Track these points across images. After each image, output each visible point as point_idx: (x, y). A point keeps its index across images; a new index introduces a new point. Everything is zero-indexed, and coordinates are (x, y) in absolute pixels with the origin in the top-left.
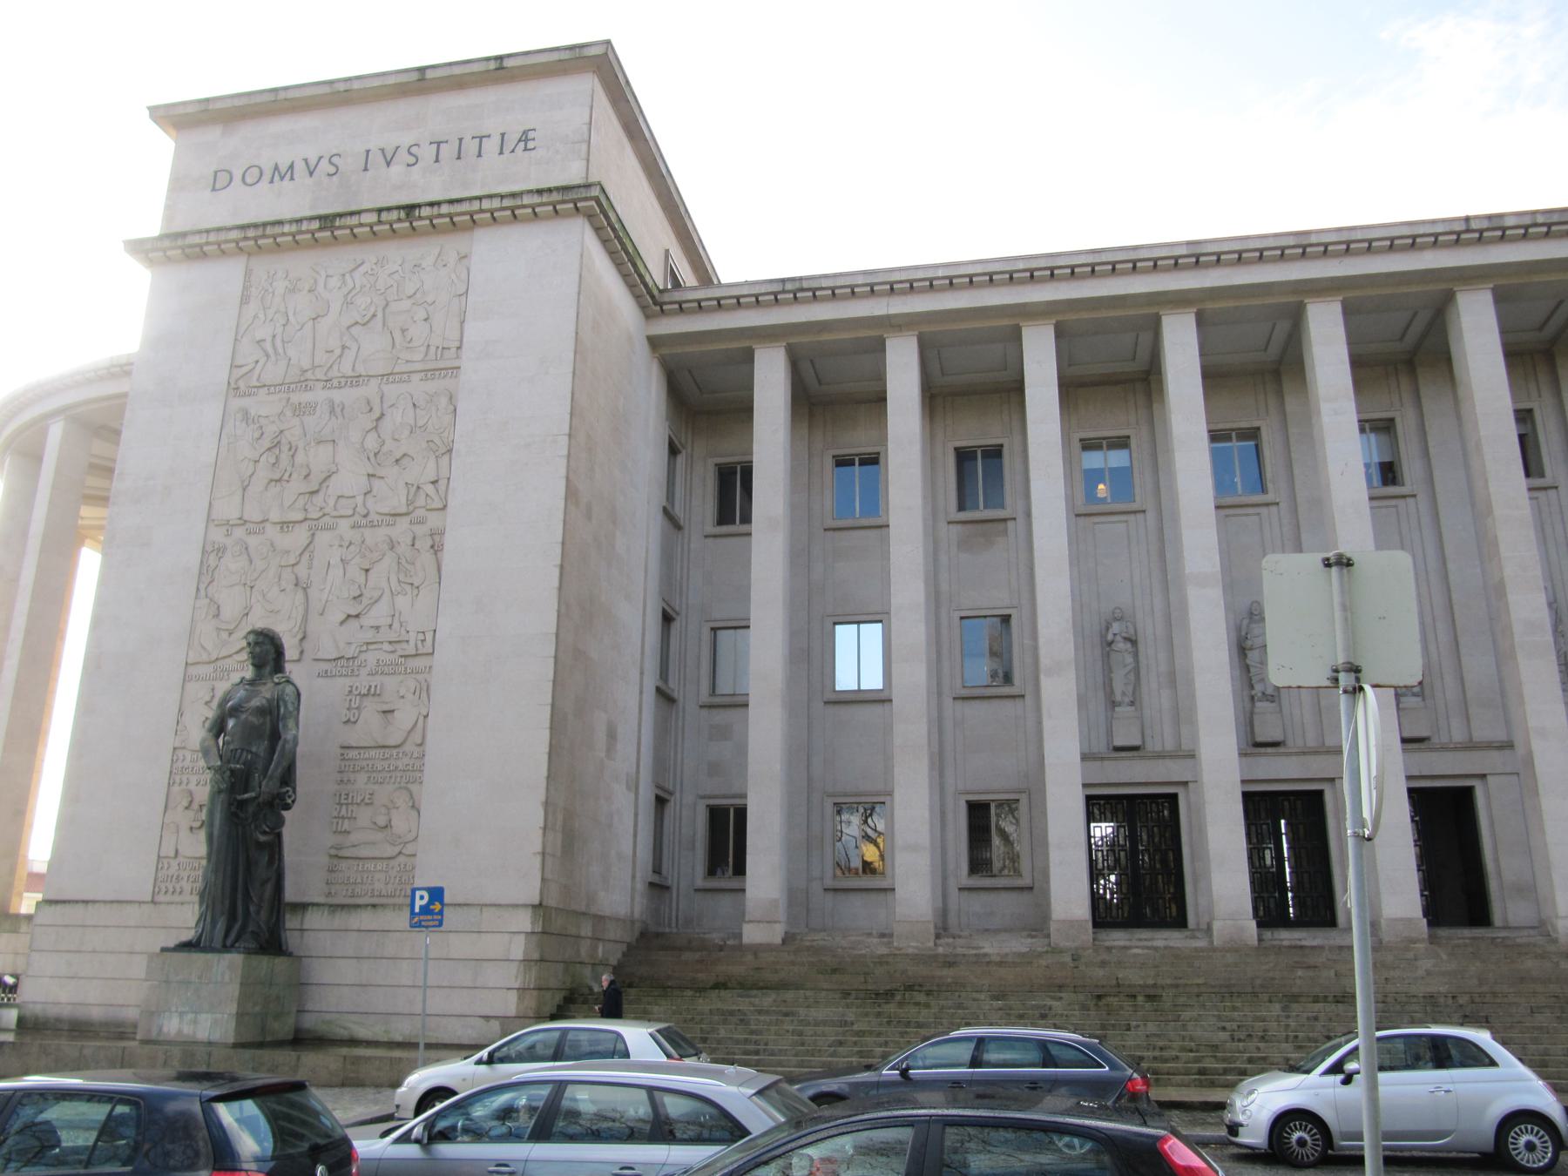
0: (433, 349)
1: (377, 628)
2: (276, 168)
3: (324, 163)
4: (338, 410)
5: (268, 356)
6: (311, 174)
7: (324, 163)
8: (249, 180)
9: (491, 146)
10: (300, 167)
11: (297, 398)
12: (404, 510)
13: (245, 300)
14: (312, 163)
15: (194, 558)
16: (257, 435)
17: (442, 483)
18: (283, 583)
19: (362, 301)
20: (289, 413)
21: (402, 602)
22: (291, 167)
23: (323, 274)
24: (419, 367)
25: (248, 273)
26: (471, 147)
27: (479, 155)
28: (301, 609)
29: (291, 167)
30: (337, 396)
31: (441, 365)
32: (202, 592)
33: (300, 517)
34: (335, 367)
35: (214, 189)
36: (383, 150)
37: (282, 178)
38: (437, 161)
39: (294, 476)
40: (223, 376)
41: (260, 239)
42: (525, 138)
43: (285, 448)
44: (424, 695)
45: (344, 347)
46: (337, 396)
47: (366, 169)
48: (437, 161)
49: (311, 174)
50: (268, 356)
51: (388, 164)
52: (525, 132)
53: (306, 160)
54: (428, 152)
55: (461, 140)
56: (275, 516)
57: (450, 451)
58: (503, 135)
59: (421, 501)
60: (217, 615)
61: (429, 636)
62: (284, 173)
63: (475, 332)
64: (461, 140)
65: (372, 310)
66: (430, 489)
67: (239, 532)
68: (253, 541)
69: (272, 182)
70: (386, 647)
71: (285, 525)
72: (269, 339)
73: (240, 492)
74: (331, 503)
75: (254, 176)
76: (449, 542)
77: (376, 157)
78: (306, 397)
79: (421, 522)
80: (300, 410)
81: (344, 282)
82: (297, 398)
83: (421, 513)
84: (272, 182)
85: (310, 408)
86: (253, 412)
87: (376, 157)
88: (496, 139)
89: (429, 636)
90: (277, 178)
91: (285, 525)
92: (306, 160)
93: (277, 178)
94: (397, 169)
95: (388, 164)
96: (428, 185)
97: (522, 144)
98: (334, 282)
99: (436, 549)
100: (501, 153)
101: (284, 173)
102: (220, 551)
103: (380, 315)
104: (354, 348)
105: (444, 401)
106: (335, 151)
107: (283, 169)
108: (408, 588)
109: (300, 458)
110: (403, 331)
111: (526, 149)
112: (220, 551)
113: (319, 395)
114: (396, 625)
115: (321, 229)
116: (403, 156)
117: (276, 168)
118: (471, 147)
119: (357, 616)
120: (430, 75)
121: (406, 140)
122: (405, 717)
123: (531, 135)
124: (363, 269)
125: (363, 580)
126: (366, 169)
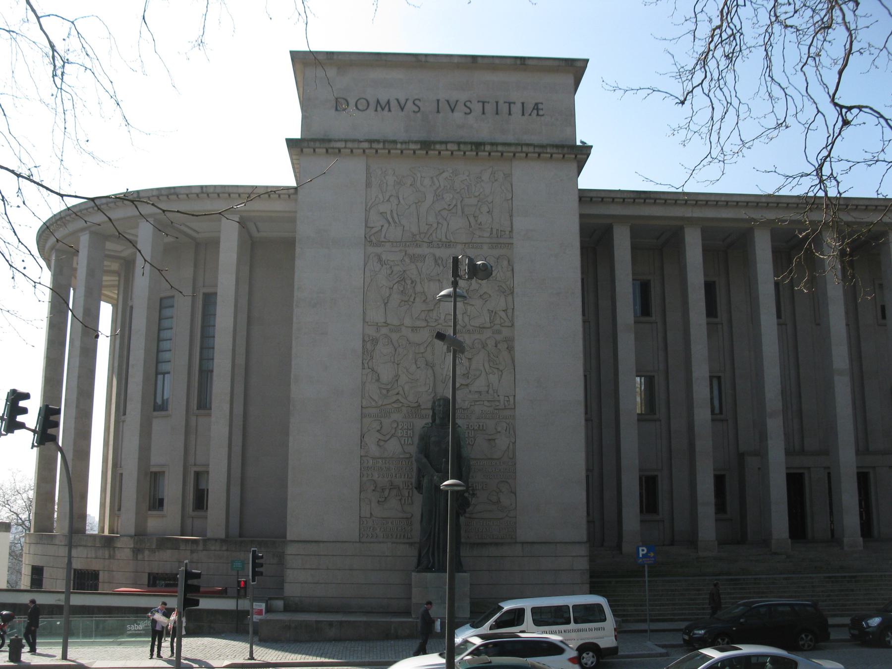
0: (494, 232)
1: (480, 392)
2: (378, 102)
3: (410, 103)
4: (440, 262)
5: (389, 223)
6: (402, 109)
7: (410, 103)
8: (360, 107)
9: (516, 109)
10: (394, 103)
11: (411, 251)
12: (488, 325)
13: (368, 185)
14: (402, 102)
15: (358, 345)
16: (389, 272)
17: (510, 311)
18: (418, 363)
19: (448, 197)
20: (407, 260)
21: (493, 378)
22: (388, 102)
23: (419, 175)
24: (488, 240)
25: (368, 168)
26: (504, 108)
27: (510, 114)
28: (432, 379)
29: (388, 102)
30: (439, 252)
31: (502, 241)
32: (366, 365)
33: (424, 324)
34: (434, 235)
35: (336, 110)
36: (448, 101)
37: (383, 109)
38: (483, 113)
39: (417, 300)
40: (362, 232)
41: (379, 147)
42: (536, 107)
43: (409, 282)
44: (512, 432)
45: (438, 223)
46: (439, 252)
47: (438, 112)
48: (483, 113)
49: (402, 109)
50: (389, 223)
51: (453, 111)
52: (536, 104)
53: (398, 100)
54: (477, 108)
55: (497, 103)
56: (407, 322)
57: (512, 293)
58: (523, 104)
59: (498, 321)
60: (378, 380)
61: (511, 399)
62: (382, 106)
63: (520, 223)
64: (497, 103)
65: (454, 202)
66: (503, 314)
67: (384, 331)
68: (394, 336)
69: (376, 110)
70: (486, 403)
71: (414, 329)
72: (389, 213)
73: (383, 306)
74: (443, 317)
75: (363, 105)
76: (518, 347)
77: (444, 106)
78: (418, 251)
79: (499, 332)
80: (414, 258)
81: (433, 182)
82: (411, 251)
83: (497, 327)
84: (376, 110)
85: (423, 258)
86: (384, 257)
87: (444, 106)
88: (519, 105)
89: (511, 399)
90: (379, 109)
91: (414, 329)
92: (398, 100)
93: (379, 109)
94: (458, 115)
95: (453, 111)
96: (484, 130)
97: (535, 111)
98: (427, 182)
99: (510, 349)
100: (523, 114)
101: (382, 106)
102: (375, 341)
103: (459, 206)
104: (445, 224)
105: (505, 263)
106: (416, 97)
107: (383, 103)
108: (496, 371)
109: (419, 288)
110: (475, 217)
111: (538, 115)
112: (375, 341)
113: (425, 250)
114: (491, 391)
115: (421, 149)
116: (460, 106)
117: (378, 102)
118: (504, 108)
119: (467, 385)
120: (480, 61)
121: (463, 97)
122: (502, 442)
123: (540, 106)
124: (445, 175)
125: (467, 364)
126: (438, 112)
